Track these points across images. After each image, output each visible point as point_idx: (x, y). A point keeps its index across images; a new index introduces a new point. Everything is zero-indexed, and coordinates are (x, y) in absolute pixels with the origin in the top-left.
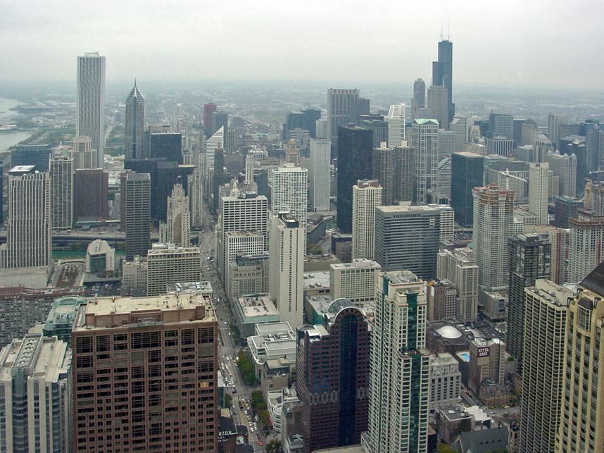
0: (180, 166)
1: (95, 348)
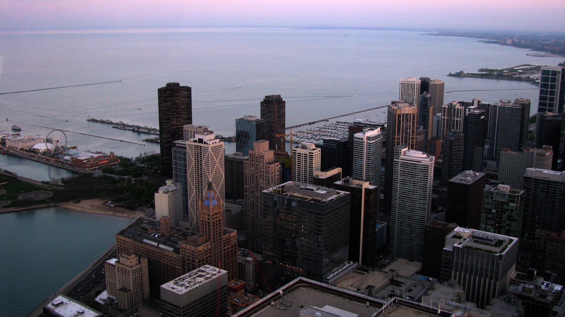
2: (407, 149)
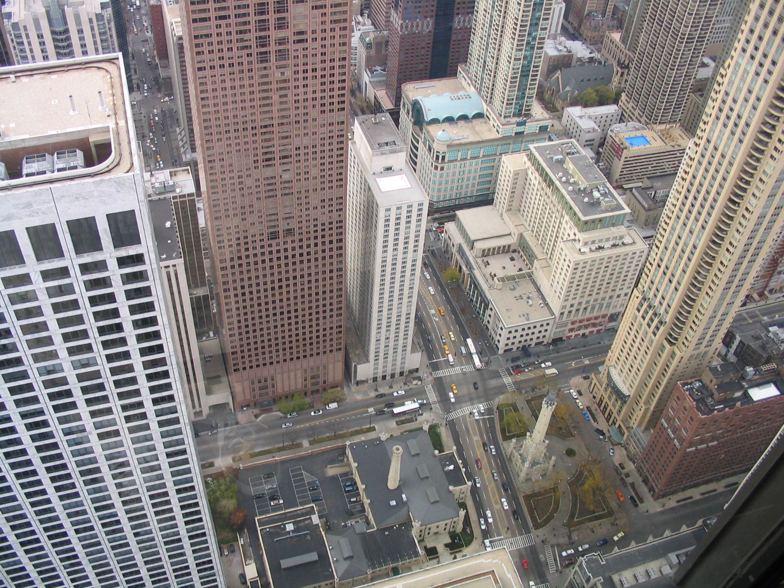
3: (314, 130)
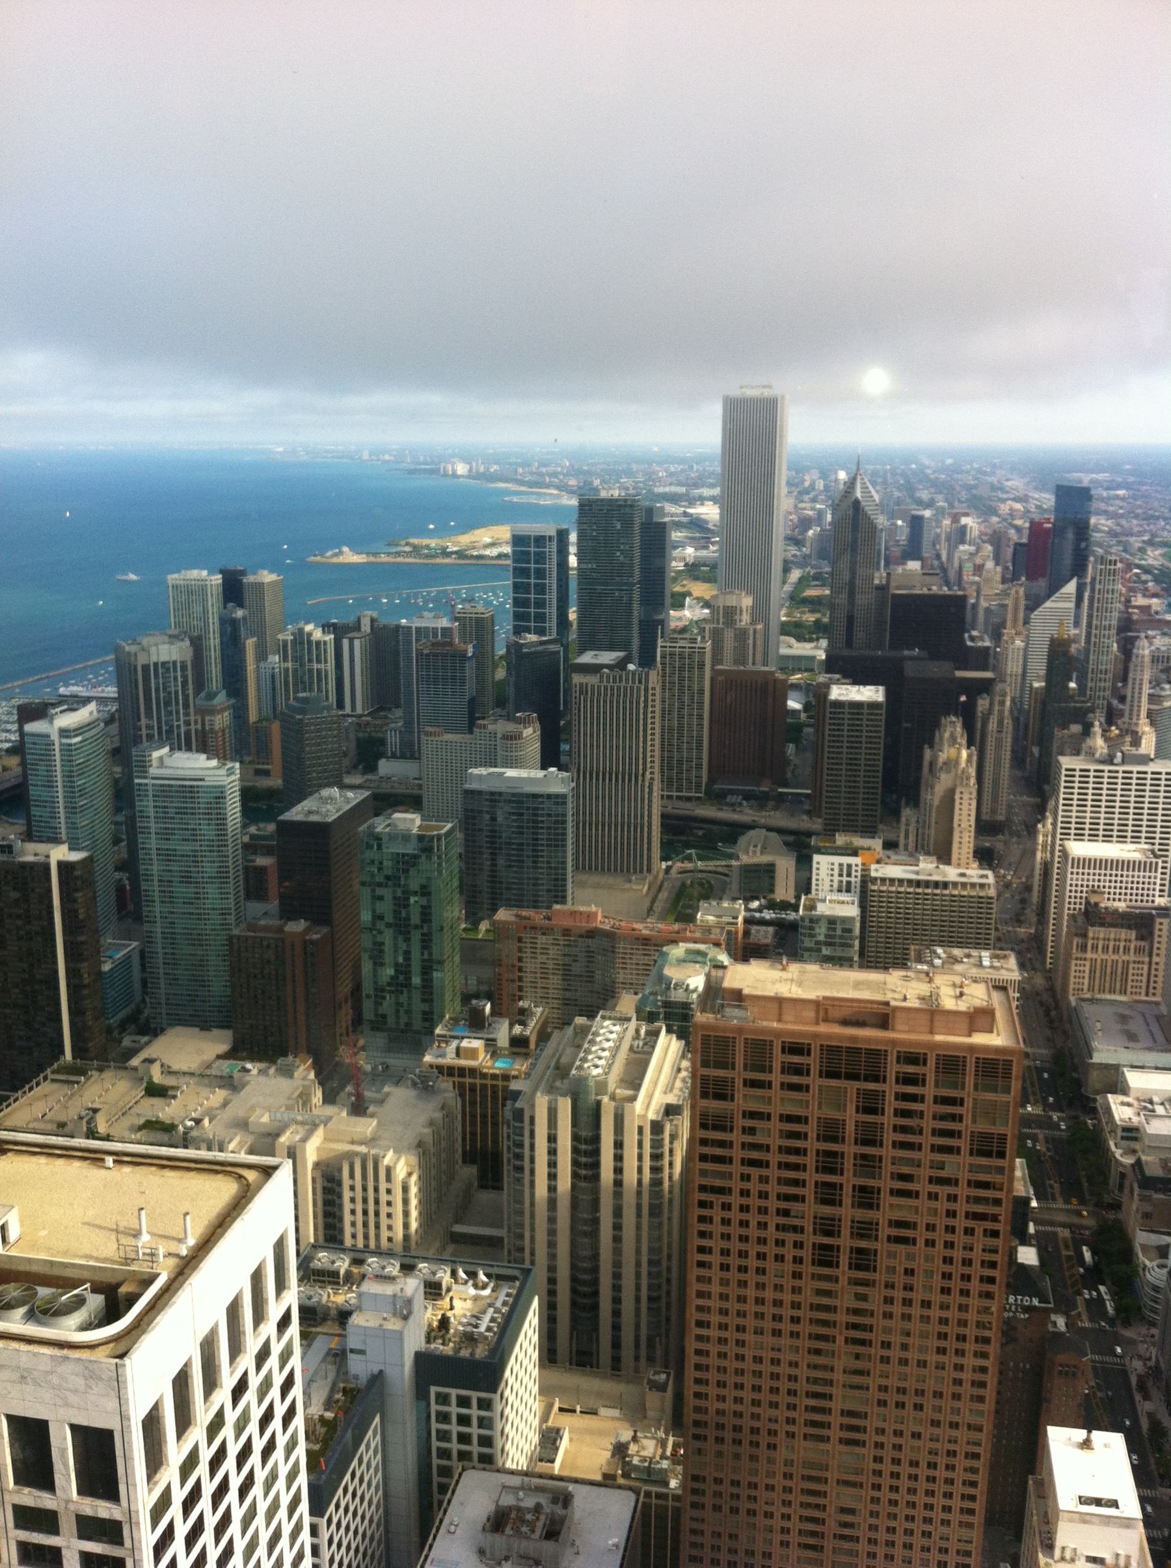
0: (960, 674)
1: (739, 1060)
2: (166, 750)
3: (917, 1429)
